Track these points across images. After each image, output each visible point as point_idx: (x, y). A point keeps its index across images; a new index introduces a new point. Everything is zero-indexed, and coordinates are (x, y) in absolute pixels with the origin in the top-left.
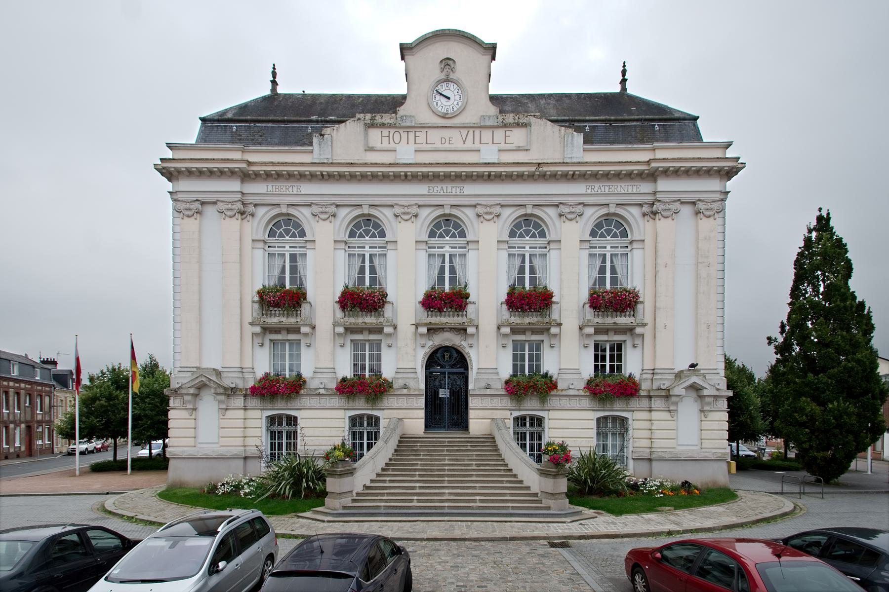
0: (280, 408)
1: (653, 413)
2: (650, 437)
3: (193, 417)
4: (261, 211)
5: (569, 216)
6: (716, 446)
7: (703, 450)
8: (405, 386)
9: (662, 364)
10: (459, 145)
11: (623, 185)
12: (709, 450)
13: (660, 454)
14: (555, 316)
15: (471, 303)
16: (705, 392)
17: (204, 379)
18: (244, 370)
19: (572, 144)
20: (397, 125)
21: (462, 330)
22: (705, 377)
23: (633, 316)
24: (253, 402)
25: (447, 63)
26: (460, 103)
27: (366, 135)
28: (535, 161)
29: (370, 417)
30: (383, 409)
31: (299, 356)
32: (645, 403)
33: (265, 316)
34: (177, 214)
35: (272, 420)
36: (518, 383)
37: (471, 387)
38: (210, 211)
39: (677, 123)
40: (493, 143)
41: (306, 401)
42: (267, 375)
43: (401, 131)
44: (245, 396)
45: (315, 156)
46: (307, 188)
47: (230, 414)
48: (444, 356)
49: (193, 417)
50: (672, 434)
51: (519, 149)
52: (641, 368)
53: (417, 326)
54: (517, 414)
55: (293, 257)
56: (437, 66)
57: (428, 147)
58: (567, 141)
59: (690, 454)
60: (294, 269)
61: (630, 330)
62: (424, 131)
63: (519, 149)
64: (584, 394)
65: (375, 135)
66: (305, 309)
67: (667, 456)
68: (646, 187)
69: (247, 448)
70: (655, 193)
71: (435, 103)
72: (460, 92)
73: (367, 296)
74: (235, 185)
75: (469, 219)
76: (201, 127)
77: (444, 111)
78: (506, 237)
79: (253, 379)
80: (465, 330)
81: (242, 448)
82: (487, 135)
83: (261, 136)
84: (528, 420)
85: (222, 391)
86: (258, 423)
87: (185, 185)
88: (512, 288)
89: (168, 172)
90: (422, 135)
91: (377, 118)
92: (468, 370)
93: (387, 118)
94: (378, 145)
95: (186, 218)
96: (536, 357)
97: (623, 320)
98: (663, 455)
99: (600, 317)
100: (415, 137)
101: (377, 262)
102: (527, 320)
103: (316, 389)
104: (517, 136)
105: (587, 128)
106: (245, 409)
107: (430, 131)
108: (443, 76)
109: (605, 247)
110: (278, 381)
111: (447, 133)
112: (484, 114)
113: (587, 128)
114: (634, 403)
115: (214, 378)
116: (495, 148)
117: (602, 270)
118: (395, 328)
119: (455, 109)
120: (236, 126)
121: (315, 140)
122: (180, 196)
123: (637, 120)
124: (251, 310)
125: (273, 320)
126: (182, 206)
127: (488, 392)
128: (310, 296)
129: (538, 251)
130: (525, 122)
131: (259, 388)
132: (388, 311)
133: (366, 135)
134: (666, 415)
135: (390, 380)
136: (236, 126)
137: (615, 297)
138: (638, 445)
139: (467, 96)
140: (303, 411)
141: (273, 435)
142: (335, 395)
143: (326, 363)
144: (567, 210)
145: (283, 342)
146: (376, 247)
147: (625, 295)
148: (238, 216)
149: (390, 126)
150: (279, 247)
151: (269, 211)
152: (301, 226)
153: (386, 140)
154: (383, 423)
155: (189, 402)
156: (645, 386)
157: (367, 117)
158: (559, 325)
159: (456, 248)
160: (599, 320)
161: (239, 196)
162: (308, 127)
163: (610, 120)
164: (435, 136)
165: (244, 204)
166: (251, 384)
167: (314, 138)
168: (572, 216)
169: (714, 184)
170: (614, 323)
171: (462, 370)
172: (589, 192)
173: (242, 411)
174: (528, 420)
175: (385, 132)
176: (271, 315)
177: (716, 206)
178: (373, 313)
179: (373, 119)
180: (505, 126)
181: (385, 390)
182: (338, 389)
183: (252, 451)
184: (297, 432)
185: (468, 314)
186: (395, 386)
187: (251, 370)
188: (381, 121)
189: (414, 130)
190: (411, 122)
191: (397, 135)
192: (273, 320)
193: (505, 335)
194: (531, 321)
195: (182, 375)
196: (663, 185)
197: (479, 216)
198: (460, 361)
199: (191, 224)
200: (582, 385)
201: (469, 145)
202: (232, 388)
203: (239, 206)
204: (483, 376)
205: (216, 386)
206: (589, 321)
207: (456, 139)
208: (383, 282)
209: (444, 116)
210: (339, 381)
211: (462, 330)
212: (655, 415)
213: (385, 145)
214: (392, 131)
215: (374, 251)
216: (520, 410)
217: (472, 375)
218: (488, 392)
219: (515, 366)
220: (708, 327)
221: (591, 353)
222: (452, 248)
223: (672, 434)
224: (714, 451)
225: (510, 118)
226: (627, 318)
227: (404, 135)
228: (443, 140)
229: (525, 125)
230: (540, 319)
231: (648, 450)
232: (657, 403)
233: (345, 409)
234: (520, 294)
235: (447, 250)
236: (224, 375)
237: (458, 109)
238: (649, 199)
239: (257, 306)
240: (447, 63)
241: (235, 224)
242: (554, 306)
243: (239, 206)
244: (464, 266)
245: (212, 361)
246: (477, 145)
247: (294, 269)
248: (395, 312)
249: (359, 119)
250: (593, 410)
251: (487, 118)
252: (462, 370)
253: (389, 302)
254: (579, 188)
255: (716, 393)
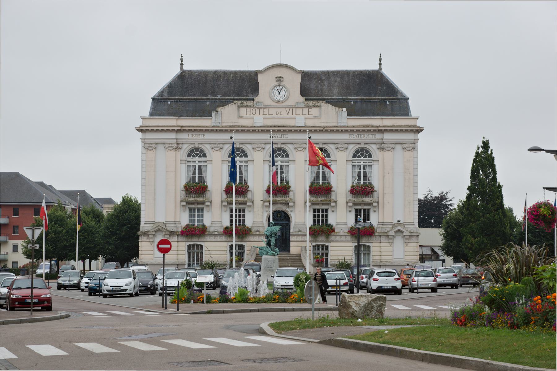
0: (195, 241)
1: (381, 243)
2: (380, 255)
3: (152, 245)
4: (185, 146)
5: (341, 149)
6: (412, 259)
7: (406, 261)
9: (387, 220)
10: (285, 115)
11: (367, 134)
12: (408, 261)
13: (384, 263)
14: (333, 197)
16: (404, 234)
17: (160, 228)
18: (176, 223)
19: (342, 116)
20: (254, 106)
22: (404, 226)
23: (372, 197)
24: (182, 238)
25: (279, 79)
26: (286, 96)
27: (239, 111)
28: (322, 126)
31: (202, 216)
32: (378, 239)
33: (187, 197)
34: (144, 149)
35: (189, 247)
38: (161, 147)
39: (398, 101)
40: (302, 114)
41: (208, 238)
43: (256, 109)
44: (178, 235)
45: (213, 121)
46: (208, 136)
50: (390, 253)
52: (378, 222)
55: (200, 167)
56: (274, 80)
57: (270, 116)
58: (339, 115)
59: (399, 263)
60: (200, 173)
61: (370, 204)
62: (268, 109)
64: (347, 234)
65: (243, 110)
67: (388, 264)
70: (382, 139)
71: (273, 96)
72: (285, 90)
73: (239, 188)
74: (173, 136)
75: (291, 150)
76: (152, 102)
77: (277, 99)
79: (181, 227)
81: (177, 260)
82: (299, 111)
83: (183, 107)
85: (168, 233)
87: (149, 136)
88: (312, 183)
89: (141, 130)
90: (266, 111)
91: (244, 103)
94: (245, 116)
95: (149, 151)
97: (367, 199)
98: (386, 263)
99: (356, 198)
100: (263, 111)
101: (243, 169)
103: (213, 232)
104: (314, 112)
105: (352, 103)
106: (178, 242)
107: (270, 109)
109: (360, 162)
112: (298, 101)
113: (352, 103)
114: (373, 239)
115: (164, 227)
116: (303, 117)
117: (359, 174)
119: (283, 99)
120: (170, 102)
121: (213, 114)
122: (147, 141)
123: (378, 99)
124: (180, 193)
125: (192, 199)
126: (147, 145)
128: (209, 188)
130: (318, 105)
131: (185, 231)
133: (239, 111)
134: (388, 244)
136: (170, 102)
137: (362, 189)
138: (374, 259)
139: (289, 93)
140: (206, 243)
141: (189, 254)
143: (217, 219)
144: (340, 146)
146: (243, 162)
147: (366, 188)
149: (251, 107)
151: (188, 146)
153: (248, 113)
156: (378, 230)
157: (239, 103)
158: (336, 202)
160: (355, 199)
161: (175, 140)
162: (207, 102)
163: (364, 99)
164: (273, 111)
165: (177, 144)
166: (180, 230)
167: (213, 113)
168: (342, 149)
169: (411, 136)
170: (362, 201)
172: (351, 138)
173: (176, 243)
175: (248, 109)
176: (190, 197)
177: (412, 146)
178: (242, 196)
179: (242, 103)
183: (181, 261)
184: (202, 253)
189: (262, 108)
190: (261, 105)
191: (254, 110)
192: (192, 199)
194: (321, 200)
195: (146, 225)
196: (386, 136)
199: (151, 154)
200: (347, 230)
201: (290, 115)
202: (172, 232)
203: (175, 145)
206: (350, 200)
208: (246, 179)
212: (382, 244)
213: (248, 115)
214: (252, 109)
220: (409, 203)
223: (390, 253)
224: (410, 261)
225: (311, 103)
226: (369, 198)
229: (319, 107)
230: (325, 199)
231: (379, 261)
232: (383, 239)
236: (167, 225)
237: (284, 99)
238: (380, 141)
239: (184, 193)
240: (279, 79)
241: (172, 153)
242: (333, 193)
243: (175, 145)
245: (160, 219)
246: (294, 116)
247: (200, 173)
249: (235, 103)
250: (353, 242)
251: (299, 103)
253: (250, 191)
254: (346, 136)
255: (410, 234)
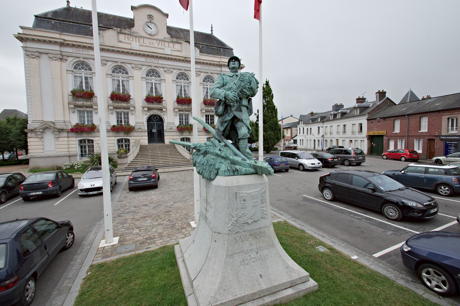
0: (85, 137)
3: (42, 141)
4: (70, 59)
8: (140, 128)
10: (157, 46)
11: (212, 67)
15: (164, 101)
21: (161, 110)
24: (71, 134)
25: (150, 16)
27: (118, 36)
29: (125, 140)
30: (131, 136)
33: (75, 101)
35: (81, 141)
36: (181, 127)
37: (165, 128)
42: (77, 124)
43: (133, 37)
44: (68, 132)
47: (60, 139)
48: (154, 118)
49: (42, 141)
51: (178, 51)
53: (143, 108)
54: (181, 137)
55: (86, 78)
60: (87, 83)
62: (142, 39)
63: (178, 51)
65: (122, 37)
66: (94, 99)
68: (219, 69)
69: (70, 152)
70: (221, 71)
72: (156, 27)
74: (57, 48)
75: (161, 71)
77: (150, 33)
78: (175, 79)
80: (162, 109)
81: (68, 152)
82: (166, 44)
83: (67, 28)
84: (185, 139)
86: (75, 143)
90: (141, 40)
92: (163, 123)
93: (127, 31)
94: (124, 41)
96: (187, 119)
101: (125, 83)
102: (184, 107)
104: (177, 46)
106: (68, 137)
107: (145, 39)
108: (149, 20)
110: (84, 126)
111: (152, 41)
115: (52, 125)
116: (170, 49)
118: (135, 107)
119: (154, 33)
120: (54, 22)
123: (216, 47)
124: (68, 98)
125: (80, 103)
127: (171, 130)
129: (186, 85)
131: (75, 129)
132: (131, 102)
133: (118, 36)
135: (133, 126)
136: (54, 22)
140: (96, 138)
141: (81, 147)
142: (110, 131)
145: (84, 112)
146: (124, 78)
148: (60, 60)
149: (128, 34)
150: (79, 73)
152: (89, 66)
153: (127, 39)
154: (131, 141)
155: (40, 135)
159: (157, 81)
161: (59, 52)
163: (208, 45)
164: (147, 41)
165: (62, 55)
166: (70, 127)
171: (161, 123)
172: (202, 68)
173: (67, 138)
174: (185, 139)
175: (126, 36)
179: (121, 30)
180: (173, 42)
181: (132, 130)
182: (111, 129)
183: (72, 153)
185: (163, 104)
186: (136, 128)
187: (69, 122)
188: (124, 32)
189: (138, 38)
190: (137, 34)
192: (80, 103)
193: (176, 112)
195: (33, 124)
197: (165, 71)
198: (161, 120)
201: (160, 46)
202: (61, 129)
203: (60, 56)
204: (169, 125)
205: (54, 128)
206: (203, 108)
207: (155, 44)
208: (128, 90)
209: (150, 35)
210: (112, 126)
211: (161, 110)
213: (127, 41)
214: (129, 36)
215: (123, 79)
216: (182, 136)
217: (165, 125)
218: (171, 130)
219: (180, 122)
221: (204, 118)
222: (155, 81)
225: (175, 40)
227: (134, 39)
228: (150, 43)
229: (180, 43)
230: (188, 107)
233: (115, 137)
234: (181, 99)
235: (153, 81)
236: (56, 124)
237: (155, 33)
239: (71, 97)
243: (60, 56)
244: (160, 88)
245: (49, 118)
246: (163, 47)
247: (87, 83)
248: (134, 102)
249: (115, 30)
252: (161, 123)
253: (132, 99)
